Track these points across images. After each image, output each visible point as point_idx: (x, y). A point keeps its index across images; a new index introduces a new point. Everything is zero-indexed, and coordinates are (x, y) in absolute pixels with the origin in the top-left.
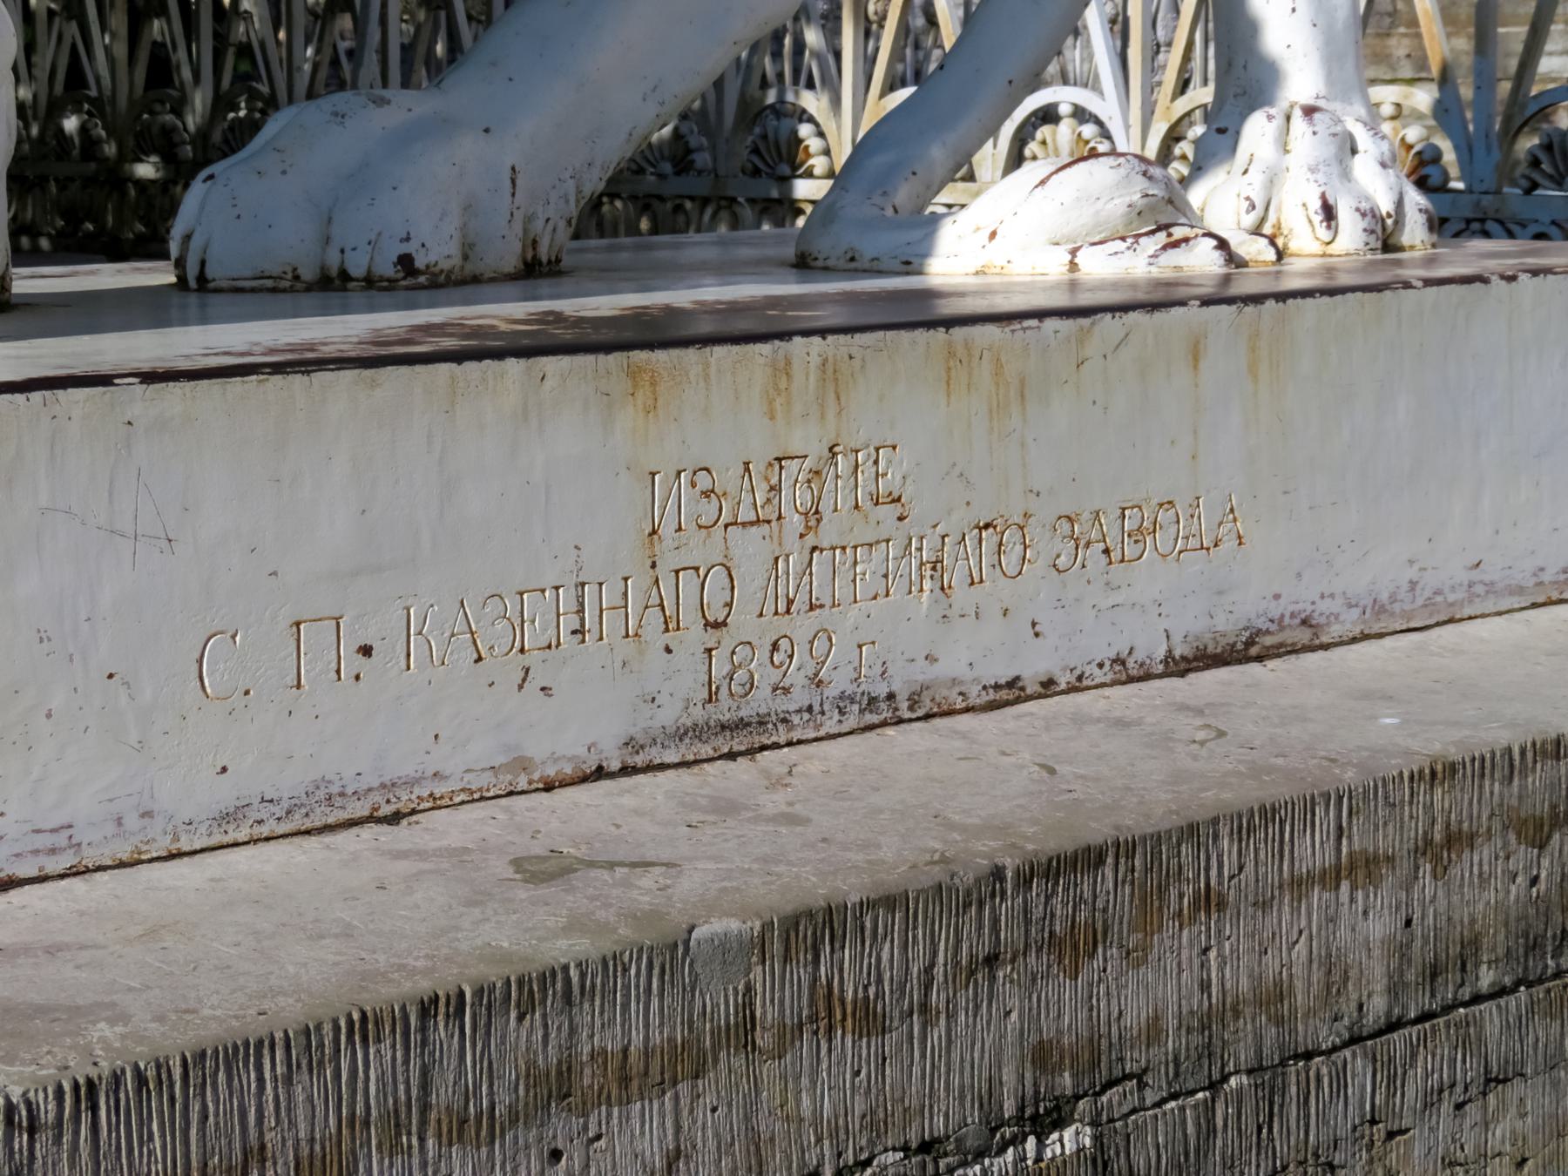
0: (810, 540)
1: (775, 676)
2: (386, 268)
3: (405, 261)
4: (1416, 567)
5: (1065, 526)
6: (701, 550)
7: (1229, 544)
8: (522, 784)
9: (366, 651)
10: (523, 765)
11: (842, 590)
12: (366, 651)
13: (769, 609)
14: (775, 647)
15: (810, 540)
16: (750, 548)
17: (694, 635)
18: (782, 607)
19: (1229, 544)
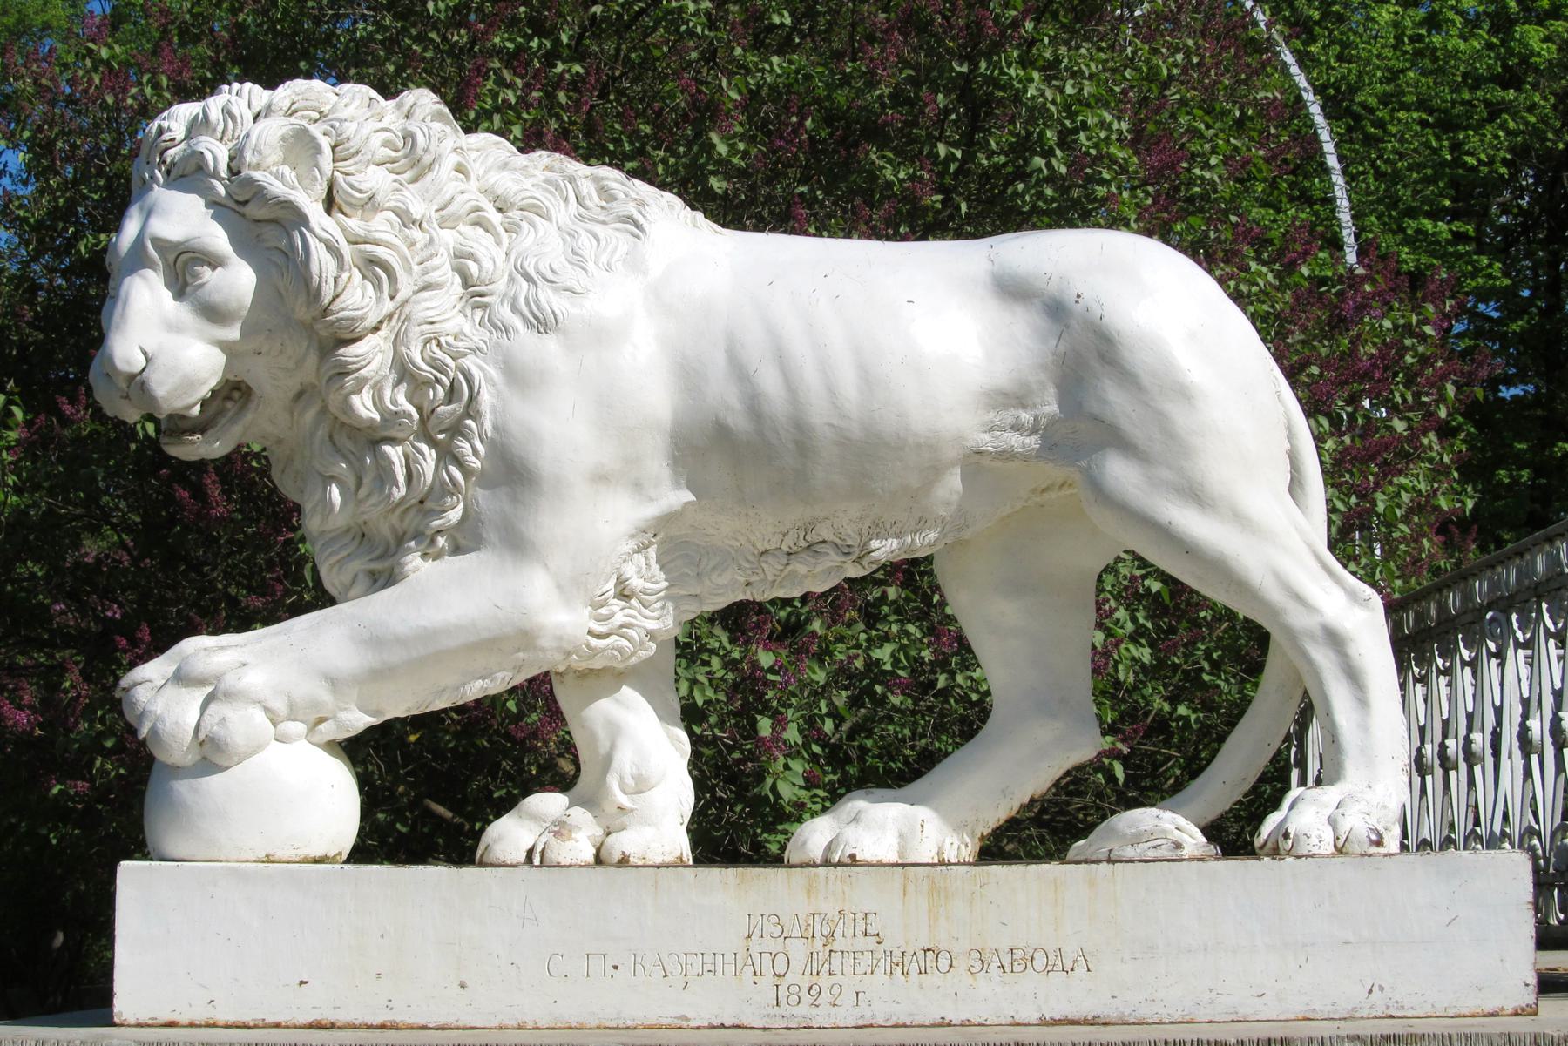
0: (828, 948)
1: (811, 1000)
2: (846, 860)
3: (853, 857)
4: (1214, 993)
5: (976, 955)
6: (771, 945)
7: (1081, 970)
8: (684, 1024)
9: (616, 967)
10: (687, 1019)
11: (848, 970)
12: (616, 967)
13: (808, 972)
14: (811, 988)
15: (828, 948)
16: (798, 949)
17: (767, 980)
18: (815, 973)
19: (1081, 970)
